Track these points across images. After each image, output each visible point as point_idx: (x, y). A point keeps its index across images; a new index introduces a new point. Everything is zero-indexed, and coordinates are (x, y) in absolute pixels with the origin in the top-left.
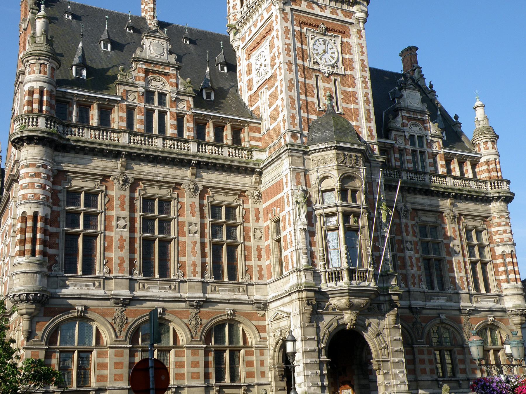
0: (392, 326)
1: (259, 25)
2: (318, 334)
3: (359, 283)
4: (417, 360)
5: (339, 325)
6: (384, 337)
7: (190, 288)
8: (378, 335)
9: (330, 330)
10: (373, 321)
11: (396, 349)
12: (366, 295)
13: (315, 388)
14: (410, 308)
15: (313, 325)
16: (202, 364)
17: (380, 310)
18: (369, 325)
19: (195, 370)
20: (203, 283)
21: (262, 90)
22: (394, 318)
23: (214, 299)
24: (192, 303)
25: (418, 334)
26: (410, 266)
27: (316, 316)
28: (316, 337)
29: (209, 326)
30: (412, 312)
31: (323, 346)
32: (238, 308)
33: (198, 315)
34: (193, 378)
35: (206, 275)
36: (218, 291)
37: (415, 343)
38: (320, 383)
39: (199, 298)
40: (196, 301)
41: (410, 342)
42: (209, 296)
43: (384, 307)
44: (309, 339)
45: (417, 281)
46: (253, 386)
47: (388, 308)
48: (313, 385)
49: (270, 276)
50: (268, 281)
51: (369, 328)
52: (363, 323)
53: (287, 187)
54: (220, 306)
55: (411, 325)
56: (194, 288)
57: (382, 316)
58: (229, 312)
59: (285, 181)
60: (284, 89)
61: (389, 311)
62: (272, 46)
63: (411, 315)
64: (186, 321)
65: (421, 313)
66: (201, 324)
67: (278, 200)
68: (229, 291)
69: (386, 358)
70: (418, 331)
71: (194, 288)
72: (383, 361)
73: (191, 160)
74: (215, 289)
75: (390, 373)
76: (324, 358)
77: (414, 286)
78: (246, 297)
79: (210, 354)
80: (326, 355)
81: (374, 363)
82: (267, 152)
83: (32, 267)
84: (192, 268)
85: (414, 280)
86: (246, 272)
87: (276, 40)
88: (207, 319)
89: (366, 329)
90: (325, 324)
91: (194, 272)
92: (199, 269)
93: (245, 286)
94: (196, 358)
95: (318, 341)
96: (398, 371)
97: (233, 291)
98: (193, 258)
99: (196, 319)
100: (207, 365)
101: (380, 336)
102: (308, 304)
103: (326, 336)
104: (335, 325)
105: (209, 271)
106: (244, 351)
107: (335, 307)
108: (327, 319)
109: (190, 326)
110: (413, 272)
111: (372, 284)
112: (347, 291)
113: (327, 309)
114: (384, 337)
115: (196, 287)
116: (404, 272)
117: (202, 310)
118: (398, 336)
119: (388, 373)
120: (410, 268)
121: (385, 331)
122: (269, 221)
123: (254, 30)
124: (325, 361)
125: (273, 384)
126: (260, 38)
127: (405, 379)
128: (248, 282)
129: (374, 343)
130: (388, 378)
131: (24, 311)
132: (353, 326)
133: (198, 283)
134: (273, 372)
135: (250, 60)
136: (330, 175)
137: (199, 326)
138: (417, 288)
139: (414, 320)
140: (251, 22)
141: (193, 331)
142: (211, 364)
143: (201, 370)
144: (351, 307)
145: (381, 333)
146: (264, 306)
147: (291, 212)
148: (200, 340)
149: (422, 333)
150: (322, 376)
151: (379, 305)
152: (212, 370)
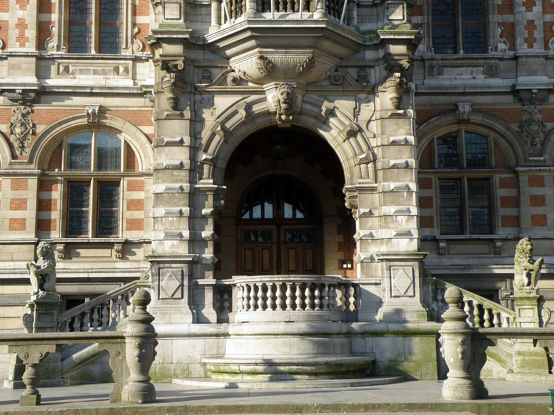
0: (389, 113)
2: (195, 135)
3: (282, 16)
4: (525, 199)
5: (250, 115)
6: (374, 141)
7: (12, 67)
8: (352, 134)
9: (228, 125)
10: (344, 106)
11: (392, 162)
12: (304, 42)
13: (175, 242)
14: (514, 92)
15: (182, 116)
16: (32, 204)
17: (362, 78)
18: (331, 113)
19: (18, 214)
20: (39, 58)
22: (394, 95)
23: (58, 87)
24: (12, 95)
25: (532, 145)
26: (524, 4)
27: (198, 97)
28: (187, 140)
29: (49, 137)
30: (521, 100)
31: (204, 157)
32: (113, 104)
33: (29, 117)
34: (12, 228)
35: (50, 45)
36: (73, 74)
37: (522, 163)
38: (186, 234)
39: (24, 85)
40: (19, 89)
41: (514, 162)
42: (53, 82)
43: (374, 74)
44: (169, 144)
45: (538, 34)
46: (139, 244)
47: (385, 73)
48: (169, 236)
51: (332, 120)
52: (316, 110)
54: (77, 101)
55: (515, 127)
56: (20, 68)
57: (369, 93)
58: (90, 111)
61: (384, 80)
63: (518, 106)
64: (5, 128)
65: (543, 101)
66: (34, 133)
68: (95, 72)
69: (369, 182)
70: (533, 139)
71: (20, 68)
72: (361, 190)
74: (67, 69)
75: (376, 213)
76: (206, 182)
77: (531, 46)
78: (129, 83)
79: (54, 187)
80: (213, 177)
81: (347, 194)
84: (17, 31)
85: (531, 34)
86: (134, 37)
88: (47, 124)
89: (325, 122)
90: (218, 112)
91: (22, 40)
92: (31, 33)
93: (130, 62)
94: (21, 194)
95: (194, 149)
96: (391, 210)
97: (104, 73)
98: (20, 14)
99: (22, 124)
100: (43, 205)
101: (359, 137)
102: (169, 70)
103: (217, 138)
104: (242, 113)
105: (56, 38)
106: (126, 182)
107: (242, 77)
108: (222, 103)
109: (12, 138)
110: (530, 16)
111: (317, 16)
112: (248, 34)
113: (223, 81)
114: (374, 141)
115: (24, 66)
116: (509, 18)
117: (37, 107)
118: (404, 132)
119: (371, 214)
120: (524, 9)
121: (374, 126)
124: (210, 190)
127: (413, 226)
128: (139, 54)
129: (345, 152)
130: (369, 225)
132: (288, 115)
133: (27, 58)
137: (30, 137)
138: (537, 49)
139: (525, 117)
141: (16, 145)
142: (56, 204)
143: (30, 214)
144: (270, 71)
145: (360, 130)
148: (30, 162)
149: (543, 143)
150: (195, 219)
151: (363, 68)
152: (56, 215)
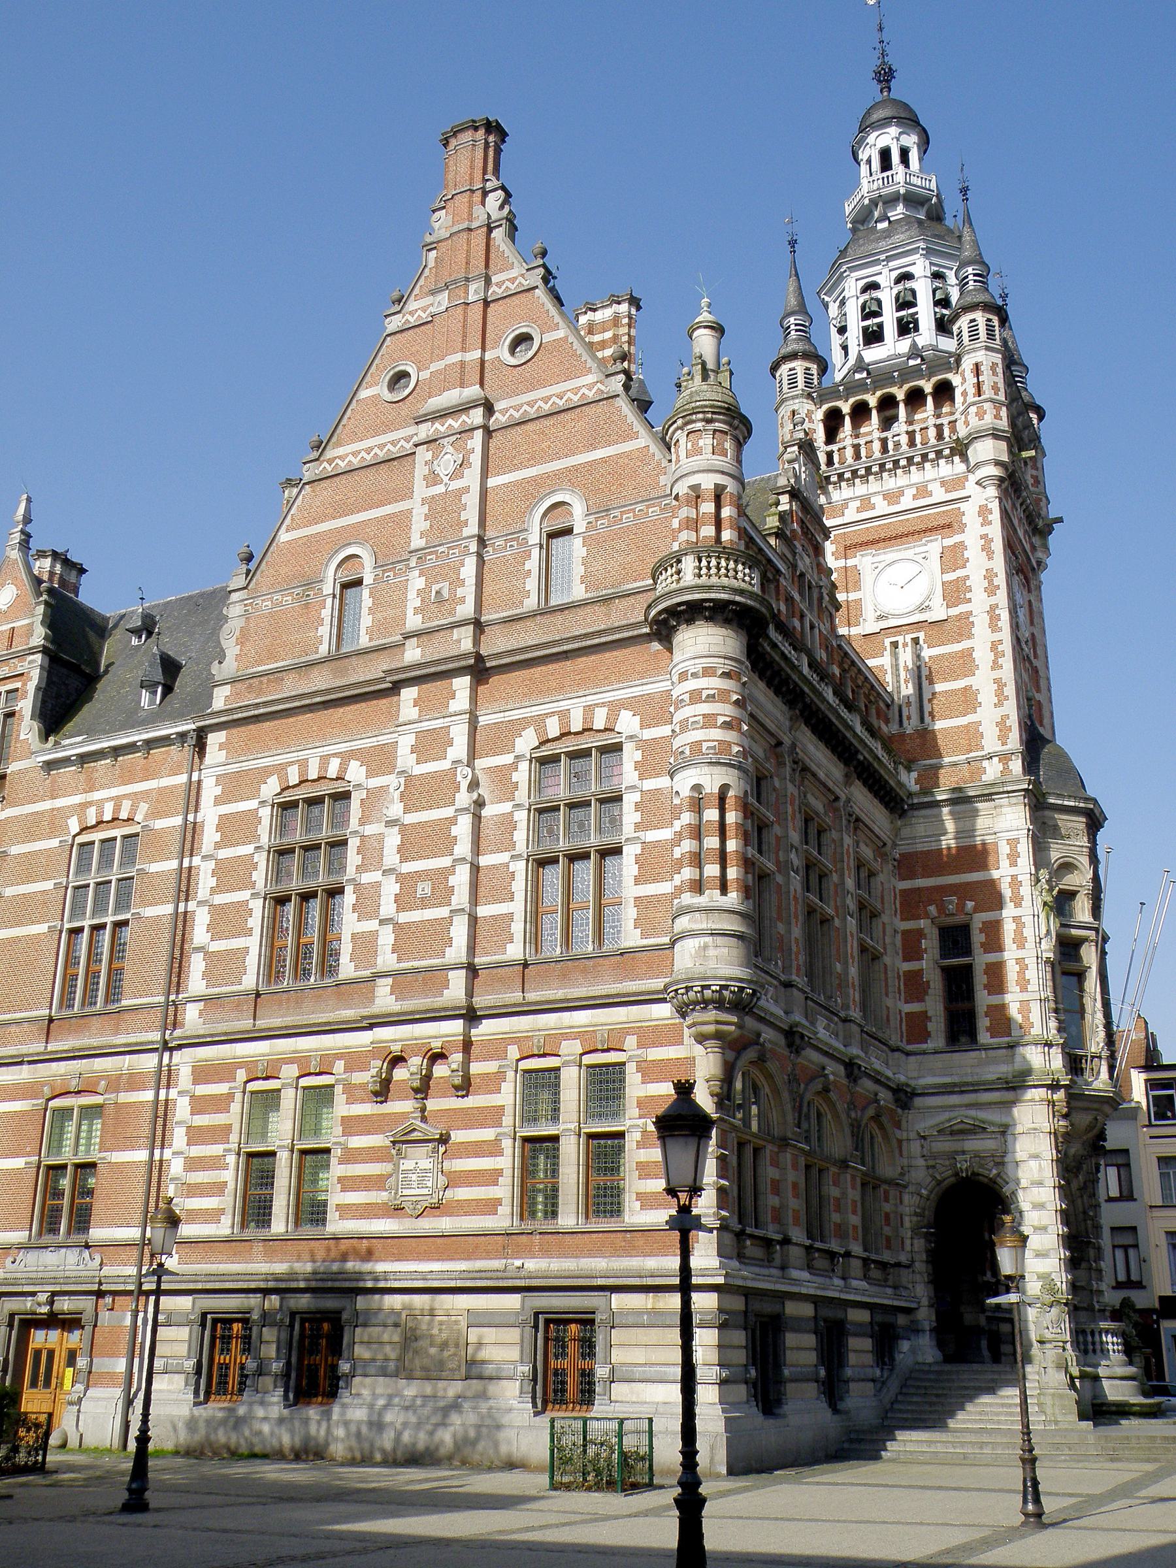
1: (907, 502)
21: (900, 639)
49: (925, 1036)
50: (910, 1048)
53: (1014, 864)
59: (1004, 849)
60: (1008, 663)
62: (953, 558)
67: (968, 884)
73: (857, 751)
82: (914, 775)
83: (748, 925)
87: (974, 552)
122: (923, 923)
123: (882, 507)
125: (920, 1266)
126: (901, 530)
131: (711, 1028)
134: (920, 1244)
135: (851, 562)
136: (1076, 862)
140: (874, 485)
146: (904, 1096)
147: (1028, 920)
